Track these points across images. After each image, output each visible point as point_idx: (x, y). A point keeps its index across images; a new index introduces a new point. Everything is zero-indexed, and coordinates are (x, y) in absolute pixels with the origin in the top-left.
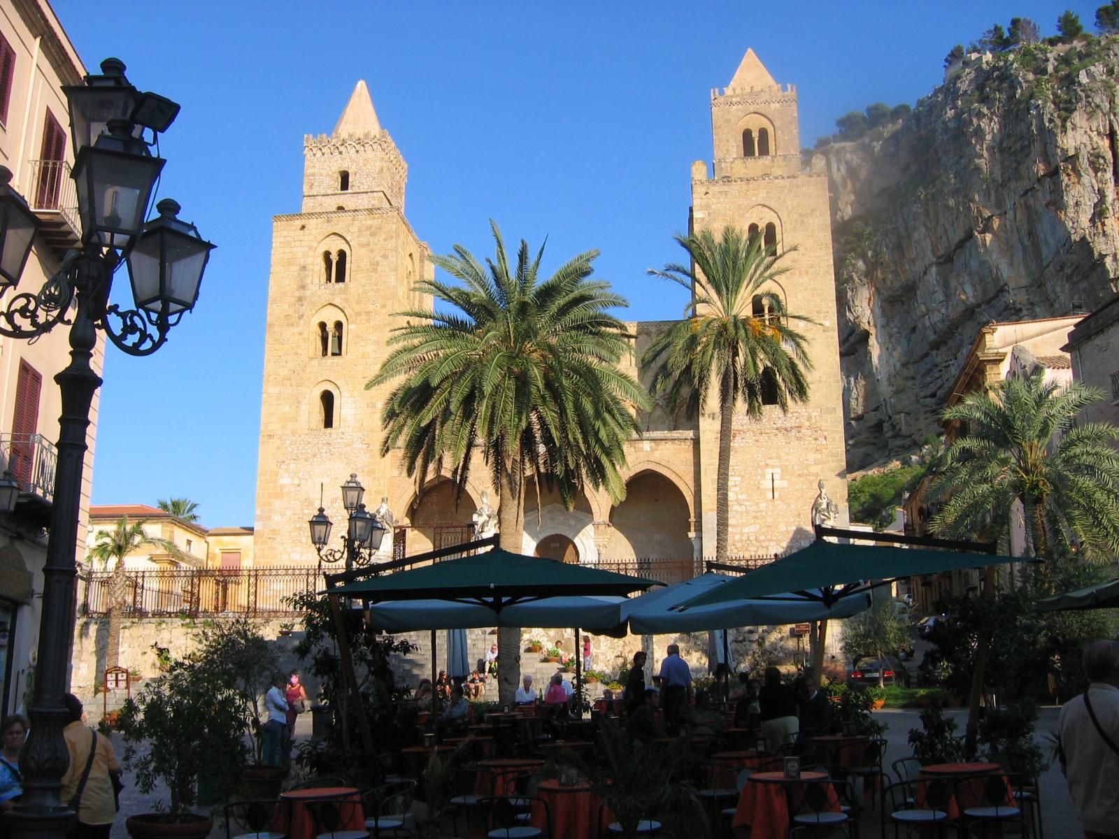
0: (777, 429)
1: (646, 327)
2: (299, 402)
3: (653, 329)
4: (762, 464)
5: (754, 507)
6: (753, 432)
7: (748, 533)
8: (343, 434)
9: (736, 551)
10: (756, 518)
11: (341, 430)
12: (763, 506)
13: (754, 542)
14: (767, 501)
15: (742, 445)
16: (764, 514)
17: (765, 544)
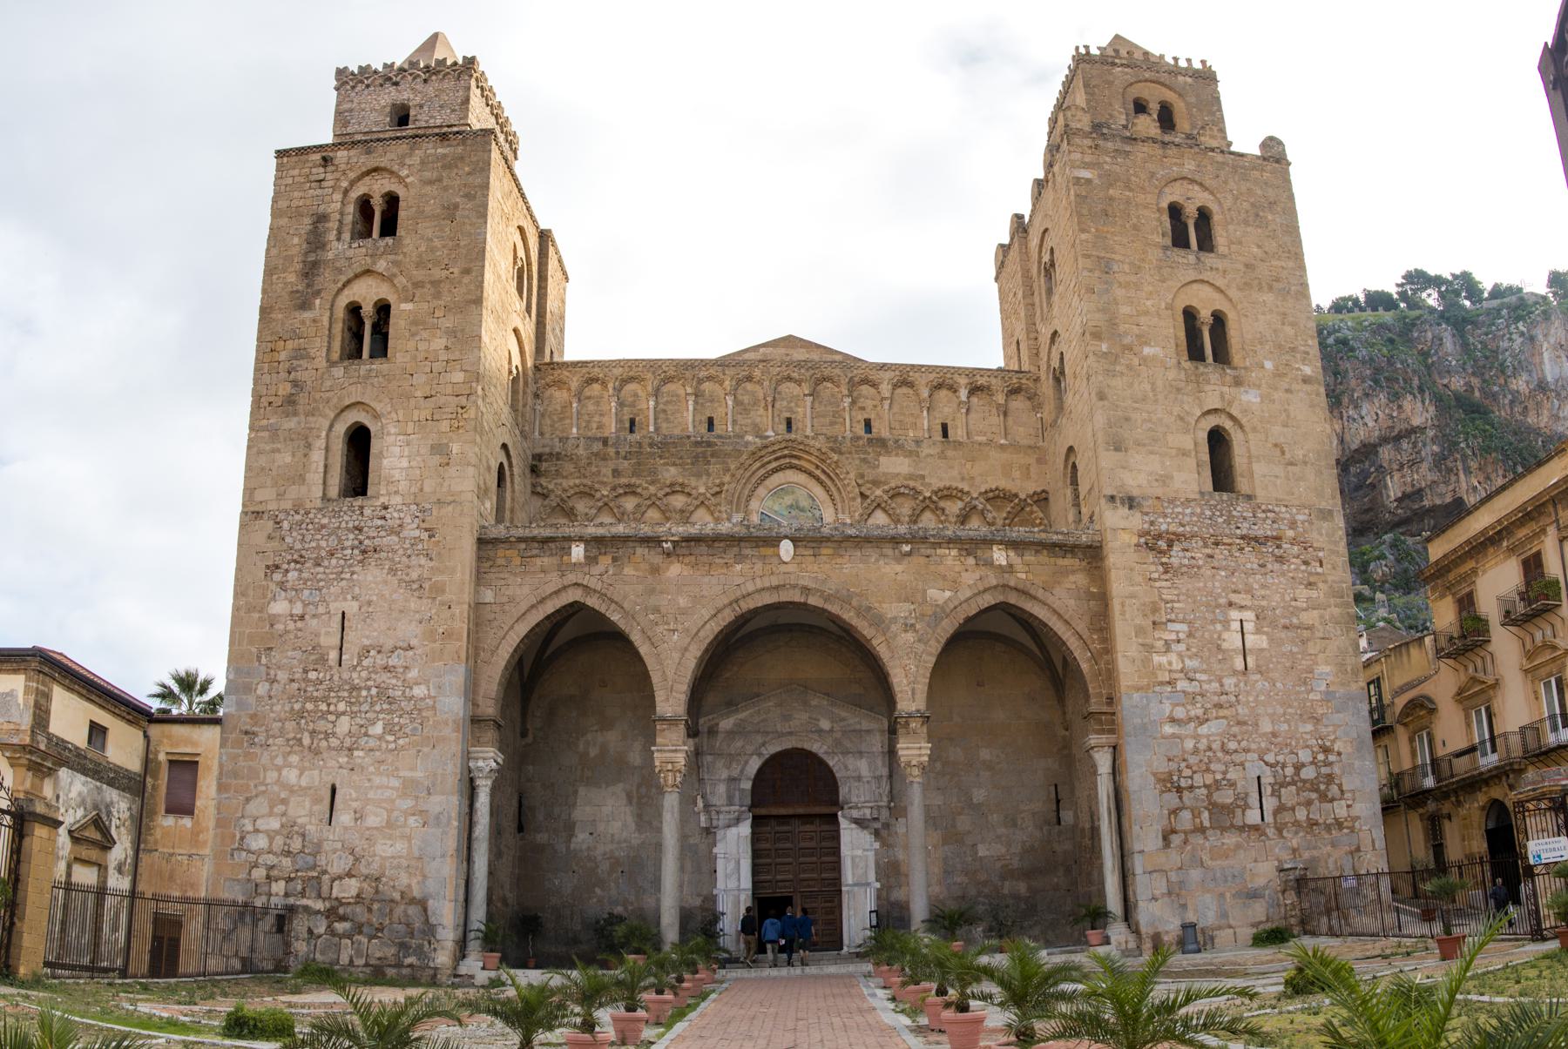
0: (1243, 537)
1: (949, 376)
2: (309, 446)
3: (963, 381)
4: (1222, 601)
5: (1215, 685)
6: (1203, 539)
7: (1208, 736)
8: (386, 508)
9: (1187, 772)
10: (1219, 706)
11: (382, 500)
12: (1229, 682)
13: (1220, 754)
14: (1235, 673)
15: (1186, 562)
16: (1234, 699)
17: (1237, 758)
